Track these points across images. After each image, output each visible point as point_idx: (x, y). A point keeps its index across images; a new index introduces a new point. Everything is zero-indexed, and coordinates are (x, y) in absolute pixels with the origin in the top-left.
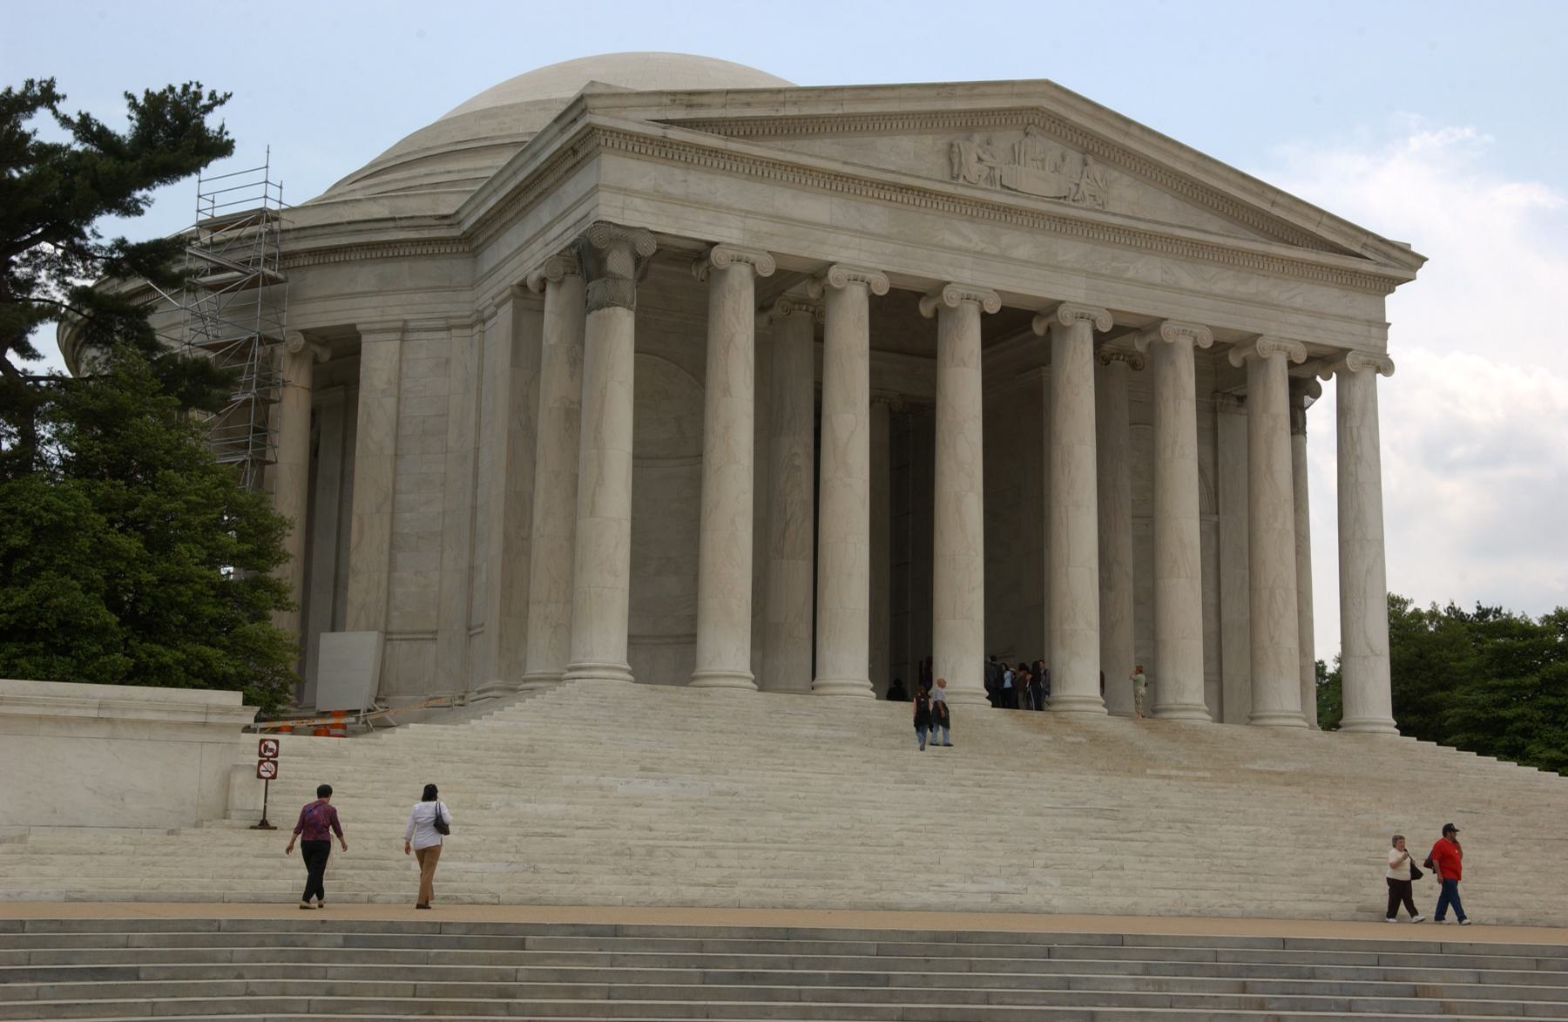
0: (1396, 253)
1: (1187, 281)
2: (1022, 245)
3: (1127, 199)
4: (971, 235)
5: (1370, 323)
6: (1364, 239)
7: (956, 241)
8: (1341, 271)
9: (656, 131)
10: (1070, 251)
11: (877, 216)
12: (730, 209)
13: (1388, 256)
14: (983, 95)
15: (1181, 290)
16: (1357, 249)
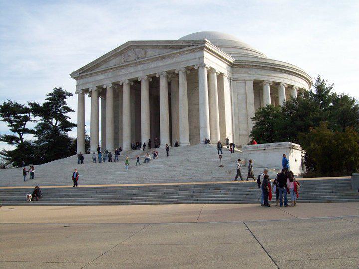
0: (199, 42)
1: (161, 64)
2: (131, 70)
3: (150, 53)
4: (124, 71)
5: (199, 58)
6: (192, 42)
7: (121, 73)
8: (190, 50)
9: (78, 76)
10: (140, 67)
11: (110, 74)
12: (91, 82)
13: (197, 43)
14: (121, 48)
15: (159, 67)
16: (191, 45)
